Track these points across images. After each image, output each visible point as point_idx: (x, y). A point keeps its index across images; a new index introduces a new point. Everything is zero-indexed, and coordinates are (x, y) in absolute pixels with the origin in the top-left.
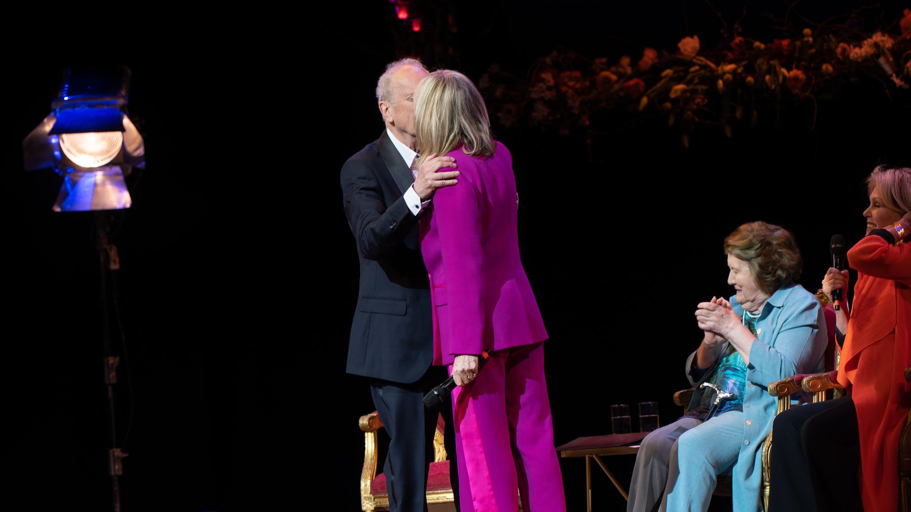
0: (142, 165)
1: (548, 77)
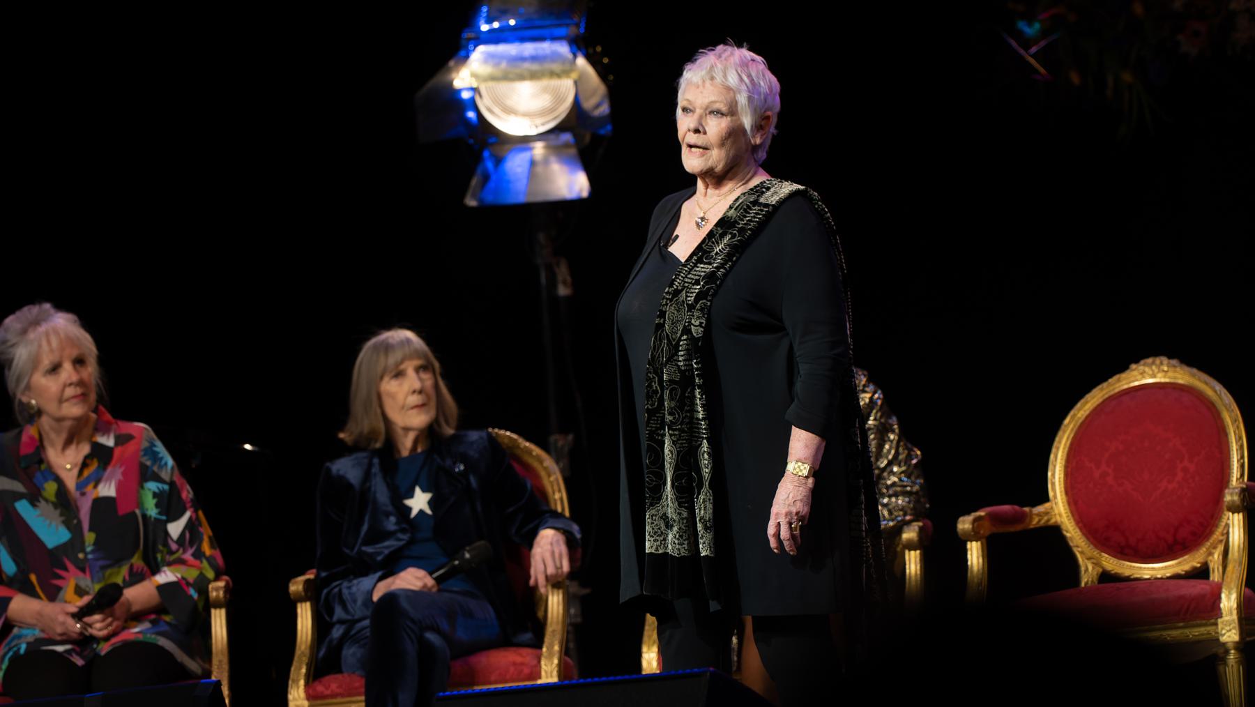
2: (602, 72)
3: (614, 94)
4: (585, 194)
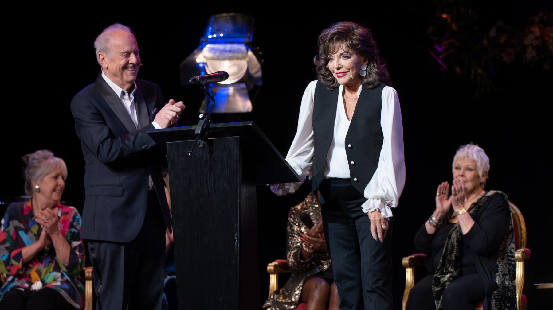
0: (260, 83)
1: (536, 30)
2: (259, 58)
3: (264, 67)
4: (250, 110)
